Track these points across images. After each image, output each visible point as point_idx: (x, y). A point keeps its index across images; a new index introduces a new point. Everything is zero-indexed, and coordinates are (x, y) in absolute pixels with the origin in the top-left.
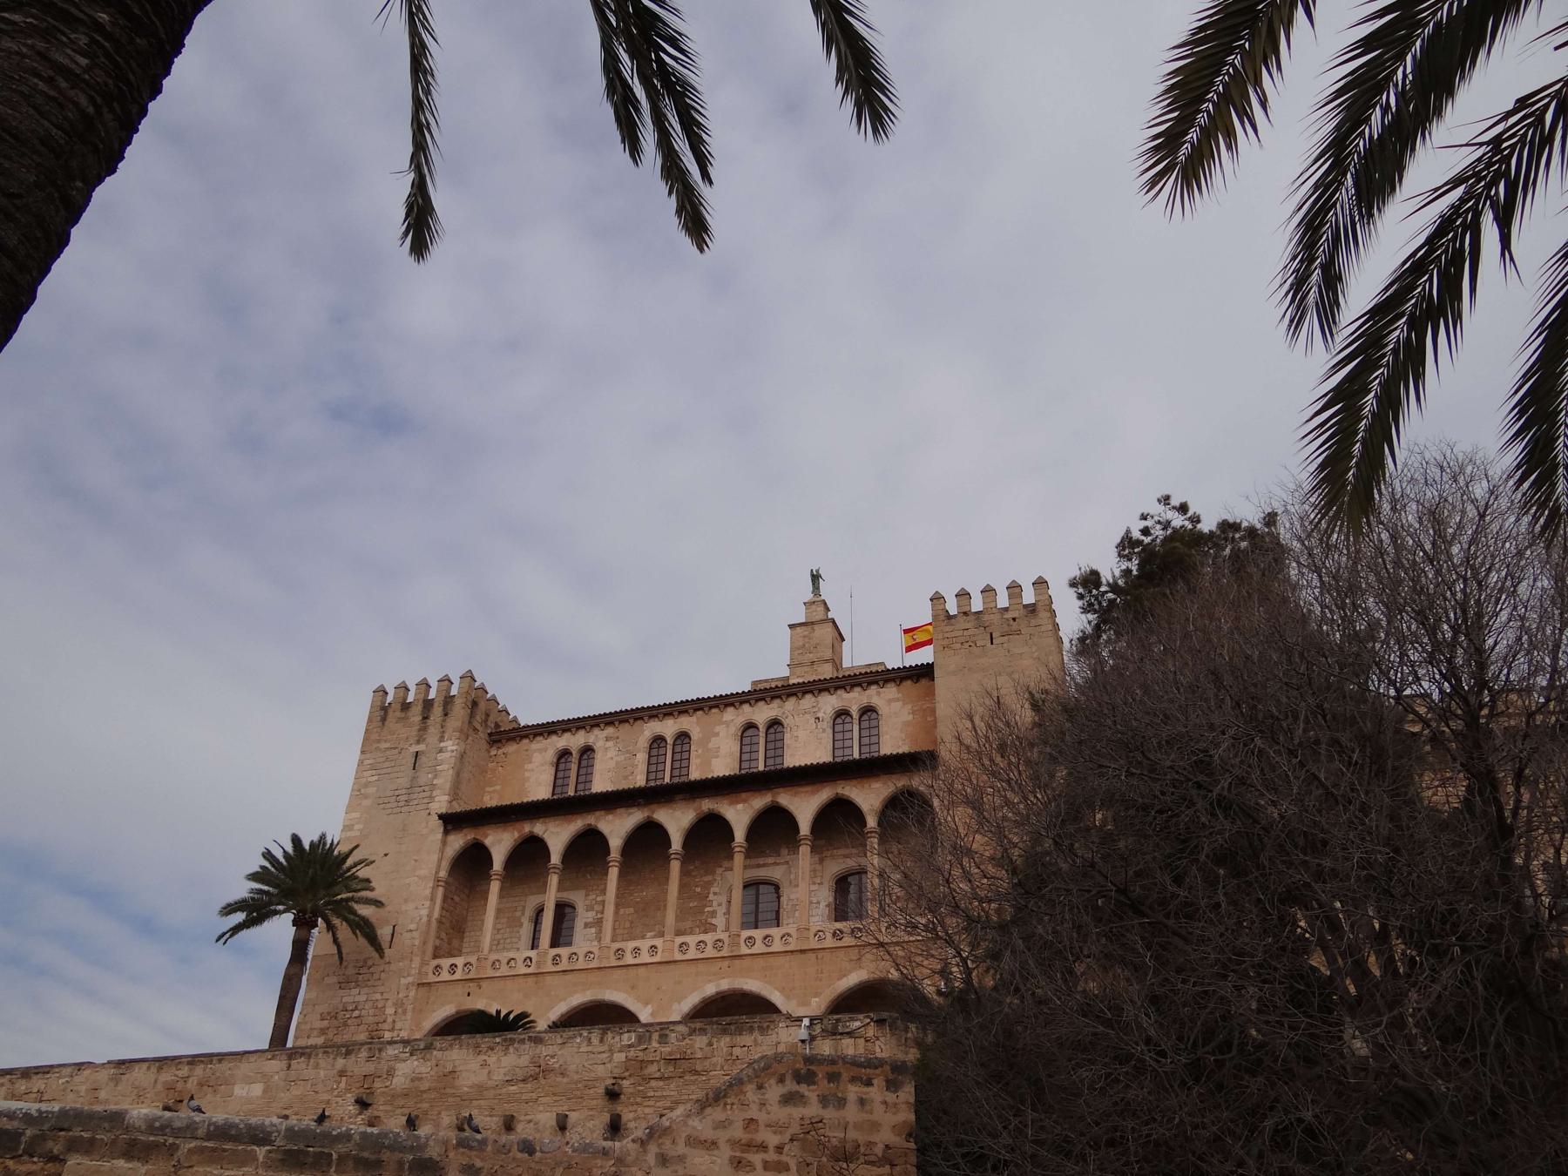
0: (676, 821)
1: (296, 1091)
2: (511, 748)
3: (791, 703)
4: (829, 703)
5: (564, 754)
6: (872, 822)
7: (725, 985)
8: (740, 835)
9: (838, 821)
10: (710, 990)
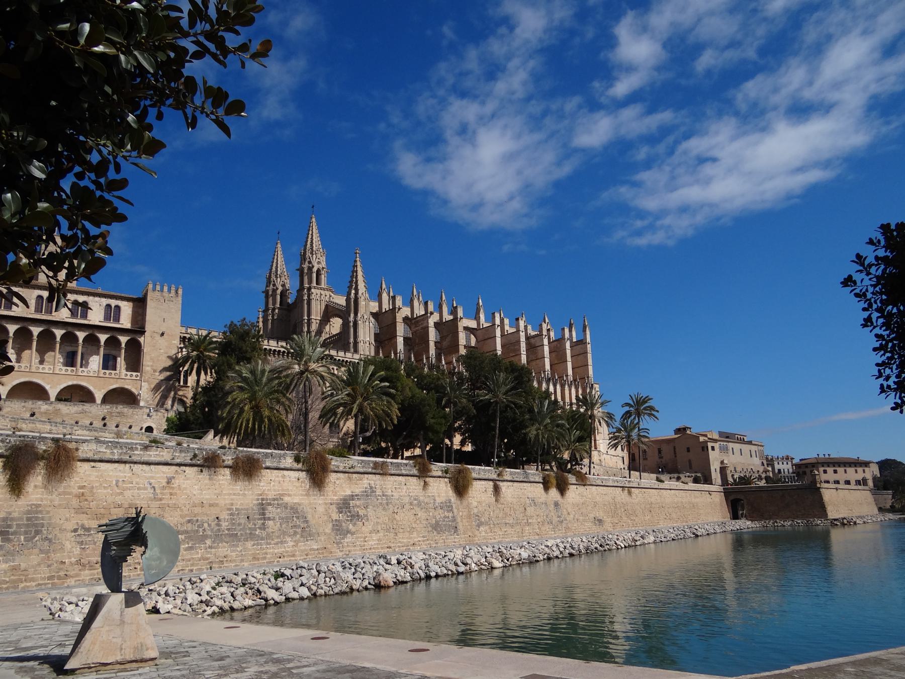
0: (59, 333)
3: (91, 298)
4: (105, 301)
7: (75, 383)
8: (81, 341)
9: (113, 342)
10: (70, 383)
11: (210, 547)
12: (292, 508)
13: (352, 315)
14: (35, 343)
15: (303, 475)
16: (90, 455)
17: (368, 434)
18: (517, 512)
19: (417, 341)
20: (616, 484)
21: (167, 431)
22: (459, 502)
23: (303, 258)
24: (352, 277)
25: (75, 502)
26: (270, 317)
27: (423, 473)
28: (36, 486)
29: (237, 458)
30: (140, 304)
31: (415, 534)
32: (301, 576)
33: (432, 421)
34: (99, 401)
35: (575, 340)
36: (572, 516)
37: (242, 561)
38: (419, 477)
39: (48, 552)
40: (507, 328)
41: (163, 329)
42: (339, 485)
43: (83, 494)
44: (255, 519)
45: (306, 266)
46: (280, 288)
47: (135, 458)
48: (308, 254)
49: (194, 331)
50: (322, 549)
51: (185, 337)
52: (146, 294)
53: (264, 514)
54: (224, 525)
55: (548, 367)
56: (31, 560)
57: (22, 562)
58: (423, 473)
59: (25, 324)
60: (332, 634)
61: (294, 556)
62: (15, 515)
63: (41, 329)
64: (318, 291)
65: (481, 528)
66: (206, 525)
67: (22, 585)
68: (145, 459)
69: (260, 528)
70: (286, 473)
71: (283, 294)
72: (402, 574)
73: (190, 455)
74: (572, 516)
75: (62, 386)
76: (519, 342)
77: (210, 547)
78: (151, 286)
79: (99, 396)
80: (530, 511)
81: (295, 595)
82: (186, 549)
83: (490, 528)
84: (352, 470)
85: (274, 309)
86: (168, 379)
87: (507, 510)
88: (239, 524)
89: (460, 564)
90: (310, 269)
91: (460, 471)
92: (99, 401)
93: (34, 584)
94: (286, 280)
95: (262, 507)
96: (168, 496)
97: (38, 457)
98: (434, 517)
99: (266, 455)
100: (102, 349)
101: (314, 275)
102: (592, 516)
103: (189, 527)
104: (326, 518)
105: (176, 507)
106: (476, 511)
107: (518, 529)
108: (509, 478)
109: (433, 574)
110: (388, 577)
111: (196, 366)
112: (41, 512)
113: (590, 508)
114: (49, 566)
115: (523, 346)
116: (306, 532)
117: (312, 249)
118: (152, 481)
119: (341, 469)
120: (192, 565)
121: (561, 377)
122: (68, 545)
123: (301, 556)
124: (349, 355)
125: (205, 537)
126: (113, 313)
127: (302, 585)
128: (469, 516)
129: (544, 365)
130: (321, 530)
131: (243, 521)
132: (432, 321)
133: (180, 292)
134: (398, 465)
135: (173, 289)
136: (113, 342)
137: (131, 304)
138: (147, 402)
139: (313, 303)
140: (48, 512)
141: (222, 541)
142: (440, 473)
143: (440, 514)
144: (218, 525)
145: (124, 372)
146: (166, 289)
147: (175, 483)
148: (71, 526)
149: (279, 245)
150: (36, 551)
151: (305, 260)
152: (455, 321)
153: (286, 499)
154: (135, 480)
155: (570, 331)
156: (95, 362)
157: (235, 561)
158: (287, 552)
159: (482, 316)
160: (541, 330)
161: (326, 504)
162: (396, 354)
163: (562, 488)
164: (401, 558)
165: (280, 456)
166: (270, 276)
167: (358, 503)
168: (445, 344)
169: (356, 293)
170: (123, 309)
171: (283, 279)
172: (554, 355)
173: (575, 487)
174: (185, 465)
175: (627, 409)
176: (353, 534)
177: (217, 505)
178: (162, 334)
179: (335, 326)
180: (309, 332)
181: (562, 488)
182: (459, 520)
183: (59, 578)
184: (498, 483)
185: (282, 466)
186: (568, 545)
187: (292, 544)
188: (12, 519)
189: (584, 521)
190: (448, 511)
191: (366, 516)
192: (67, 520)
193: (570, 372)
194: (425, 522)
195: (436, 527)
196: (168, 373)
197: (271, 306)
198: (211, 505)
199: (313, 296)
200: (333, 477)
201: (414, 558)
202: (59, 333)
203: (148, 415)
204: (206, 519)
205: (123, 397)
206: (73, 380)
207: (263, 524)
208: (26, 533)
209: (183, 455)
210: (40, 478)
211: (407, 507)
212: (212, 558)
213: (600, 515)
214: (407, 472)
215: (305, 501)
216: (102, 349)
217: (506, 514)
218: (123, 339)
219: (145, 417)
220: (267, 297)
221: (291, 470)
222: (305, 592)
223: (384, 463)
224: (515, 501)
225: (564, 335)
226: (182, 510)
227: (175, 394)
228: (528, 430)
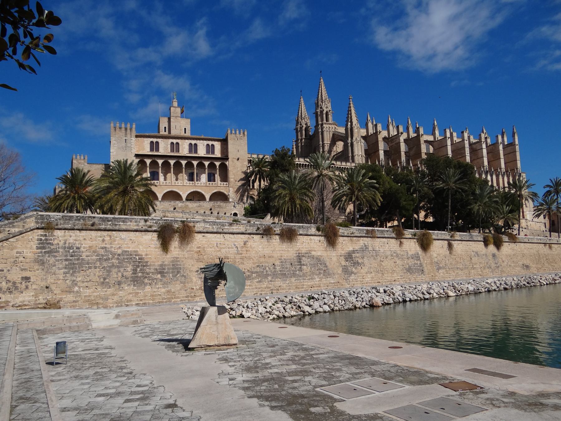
0: (184, 162)
1: (162, 206)
2: (139, 139)
3: (198, 141)
4: (206, 143)
5: (152, 142)
6: (218, 167)
7: (195, 190)
9: (212, 166)
10: (192, 190)
11: (271, 281)
12: (317, 259)
13: (350, 139)
14: (172, 169)
15: (322, 238)
16: (201, 230)
17: (363, 213)
18: (465, 261)
19: (393, 152)
20: (539, 241)
21: (245, 215)
22: (424, 254)
23: (317, 105)
24: (348, 114)
25: (196, 256)
26: (300, 145)
27: (399, 236)
28: (175, 247)
29: (283, 229)
30: (224, 142)
31: (395, 275)
32: (324, 298)
33: (404, 203)
34: (208, 199)
35: (506, 143)
36: (506, 263)
37: (289, 289)
38: (396, 239)
39: (184, 283)
40: (455, 139)
41: (238, 156)
42: (345, 245)
43: (199, 251)
44: (295, 265)
45: (319, 110)
46: (305, 126)
47: (225, 231)
48: (320, 103)
49: (255, 156)
50: (336, 283)
51: (251, 160)
52: (227, 137)
53: (300, 262)
54: (278, 268)
55: (486, 163)
56: (176, 287)
58: (399, 236)
59: (166, 159)
60: (341, 335)
61: (320, 286)
62: (166, 263)
63: (175, 161)
64: (328, 126)
65: (440, 271)
66: (267, 268)
67: (173, 300)
68: (231, 231)
69: (299, 270)
70: (312, 237)
71: (306, 129)
72: (388, 299)
73: (255, 228)
74: (506, 263)
75: (188, 192)
76: (464, 148)
77: (271, 281)
78: (229, 131)
79: (207, 197)
80: (475, 260)
81: (321, 310)
82: (257, 282)
83: (446, 271)
84: (352, 235)
85: (301, 140)
86: (243, 185)
87: (458, 259)
88: (287, 268)
89: (426, 293)
90: (322, 112)
91: (424, 235)
92: (208, 199)
93: (179, 300)
94: (307, 121)
95: (299, 257)
96: (245, 252)
97: (175, 231)
98: (408, 264)
99: (299, 227)
100: (207, 170)
101: (325, 116)
102: (521, 263)
103: (258, 269)
104: (338, 264)
105: (250, 258)
106: (436, 260)
107: (466, 271)
108: (459, 239)
109: (408, 299)
110: (378, 300)
111: (258, 176)
112: (179, 261)
113: (519, 258)
114: (186, 290)
115: (467, 150)
116: (327, 273)
117: (322, 99)
118: (236, 243)
119: (346, 234)
120: (261, 291)
121: (496, 170)
122: (194, 279)
123: (324, 287)
124: (348, 164)
125: (267, 275)
126: (210, 149)
127: (325, 304)
128: (431, 263)
129: (483, 163)
130: (335, 271)
131: (288, 266)
132: (402, 138)
133: (246, 133)
134: (382, 231)
135: (242, 132)
136: (212, 166)
137: (220, 143)
138: (233, 199)
139: (325, 133)
140: (183, 261)
141: (277, 278)
142: (410, 236)
143: (411, 262)
144: (274, 268)
145: (219, 182)
146: (238, 132)
147: (249, 244)
148: (195, 268)
149: (302, 99)
150: (178, 282)
151: (318, 107)
152: (418, 137)
153: (313, 253)
154: (226, 243)
155: (503, 137)
156: (204, 177)
157: (285, 289)
158: (316, 284)
159: (437, 133)
160: (480, 138)
161: (337, 256)
162: (379, 161)
163: (498, 244)
164: (387, 289)
165: (308, 228)
166: (298, 119)
167: (357, 255)
168: (412, 153)
169: (351, 125)
170: (216, 146)
171: (306, 120)
172: (490, 155)
173: (508, 244)
174: (253, 234)
175: (548, 189)
176: (355, 274)
177: (273, 257)
178: (238, 159)
179: (339, 146)
180: (323, 152)
181: (498, 244)
182: (425, 265)
183: (191, 297)
184: (451, 241)
185: (309, 234)
186: (503, 283)
187: (318, 279)
188: (165, 265)
189: (515, 266)
190: (417, 260)
191: (363, 263)
192: (192, 265)
193: (503, 165)
194: (401, 267)
195: (409, 270)
196: (243, 182)
197: (300, 138)
198: (270, 257)
199: (324, 129)
200: (341, 239)
201: (394, 289)
202: (184, 162)
203: (234, 206)
204: (267, 265)
205: (220, 197)
206: (194, 188)
207: (301, 268)
208: (172, 272)
209: (252, 228)
210: (177, 243)
211: (389, 257)
212: (273, 287)
213: (527, 262)
214: (388, 236)
216: (207, 170)
217: (457, 262)
218: (217, 164)
219: (233, 207)
220: (297, 132)
221: (315, 235)
222: (327, 308)
223: (373, 230)
224: (463, 253)
225: (498, 140)
226: (253, 260)
227: (248, 193)
228: (472, 206)
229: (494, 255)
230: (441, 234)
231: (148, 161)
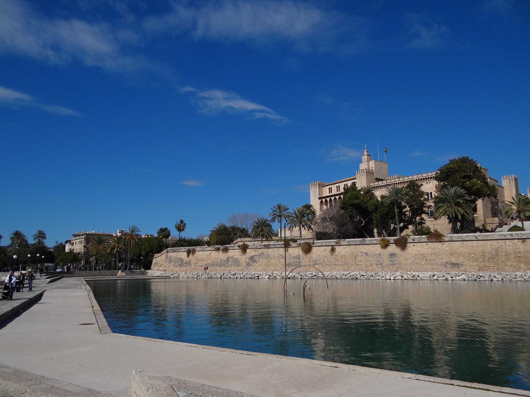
22: (304, 256)
57: (188, 268)
80: (358, 259)
102: (443, 261)
106: (314, 259)
134: (275, 245)
142: (296, 246)
173: (426, 244)
213: (460, 260)
215: (240, 257)
217: (337, 260)
229: (392, 255)
230: (326, 242)
231: (324, 200)
